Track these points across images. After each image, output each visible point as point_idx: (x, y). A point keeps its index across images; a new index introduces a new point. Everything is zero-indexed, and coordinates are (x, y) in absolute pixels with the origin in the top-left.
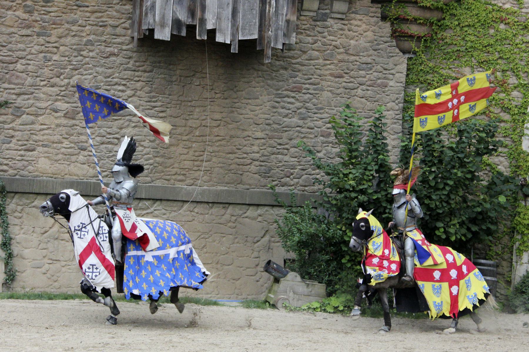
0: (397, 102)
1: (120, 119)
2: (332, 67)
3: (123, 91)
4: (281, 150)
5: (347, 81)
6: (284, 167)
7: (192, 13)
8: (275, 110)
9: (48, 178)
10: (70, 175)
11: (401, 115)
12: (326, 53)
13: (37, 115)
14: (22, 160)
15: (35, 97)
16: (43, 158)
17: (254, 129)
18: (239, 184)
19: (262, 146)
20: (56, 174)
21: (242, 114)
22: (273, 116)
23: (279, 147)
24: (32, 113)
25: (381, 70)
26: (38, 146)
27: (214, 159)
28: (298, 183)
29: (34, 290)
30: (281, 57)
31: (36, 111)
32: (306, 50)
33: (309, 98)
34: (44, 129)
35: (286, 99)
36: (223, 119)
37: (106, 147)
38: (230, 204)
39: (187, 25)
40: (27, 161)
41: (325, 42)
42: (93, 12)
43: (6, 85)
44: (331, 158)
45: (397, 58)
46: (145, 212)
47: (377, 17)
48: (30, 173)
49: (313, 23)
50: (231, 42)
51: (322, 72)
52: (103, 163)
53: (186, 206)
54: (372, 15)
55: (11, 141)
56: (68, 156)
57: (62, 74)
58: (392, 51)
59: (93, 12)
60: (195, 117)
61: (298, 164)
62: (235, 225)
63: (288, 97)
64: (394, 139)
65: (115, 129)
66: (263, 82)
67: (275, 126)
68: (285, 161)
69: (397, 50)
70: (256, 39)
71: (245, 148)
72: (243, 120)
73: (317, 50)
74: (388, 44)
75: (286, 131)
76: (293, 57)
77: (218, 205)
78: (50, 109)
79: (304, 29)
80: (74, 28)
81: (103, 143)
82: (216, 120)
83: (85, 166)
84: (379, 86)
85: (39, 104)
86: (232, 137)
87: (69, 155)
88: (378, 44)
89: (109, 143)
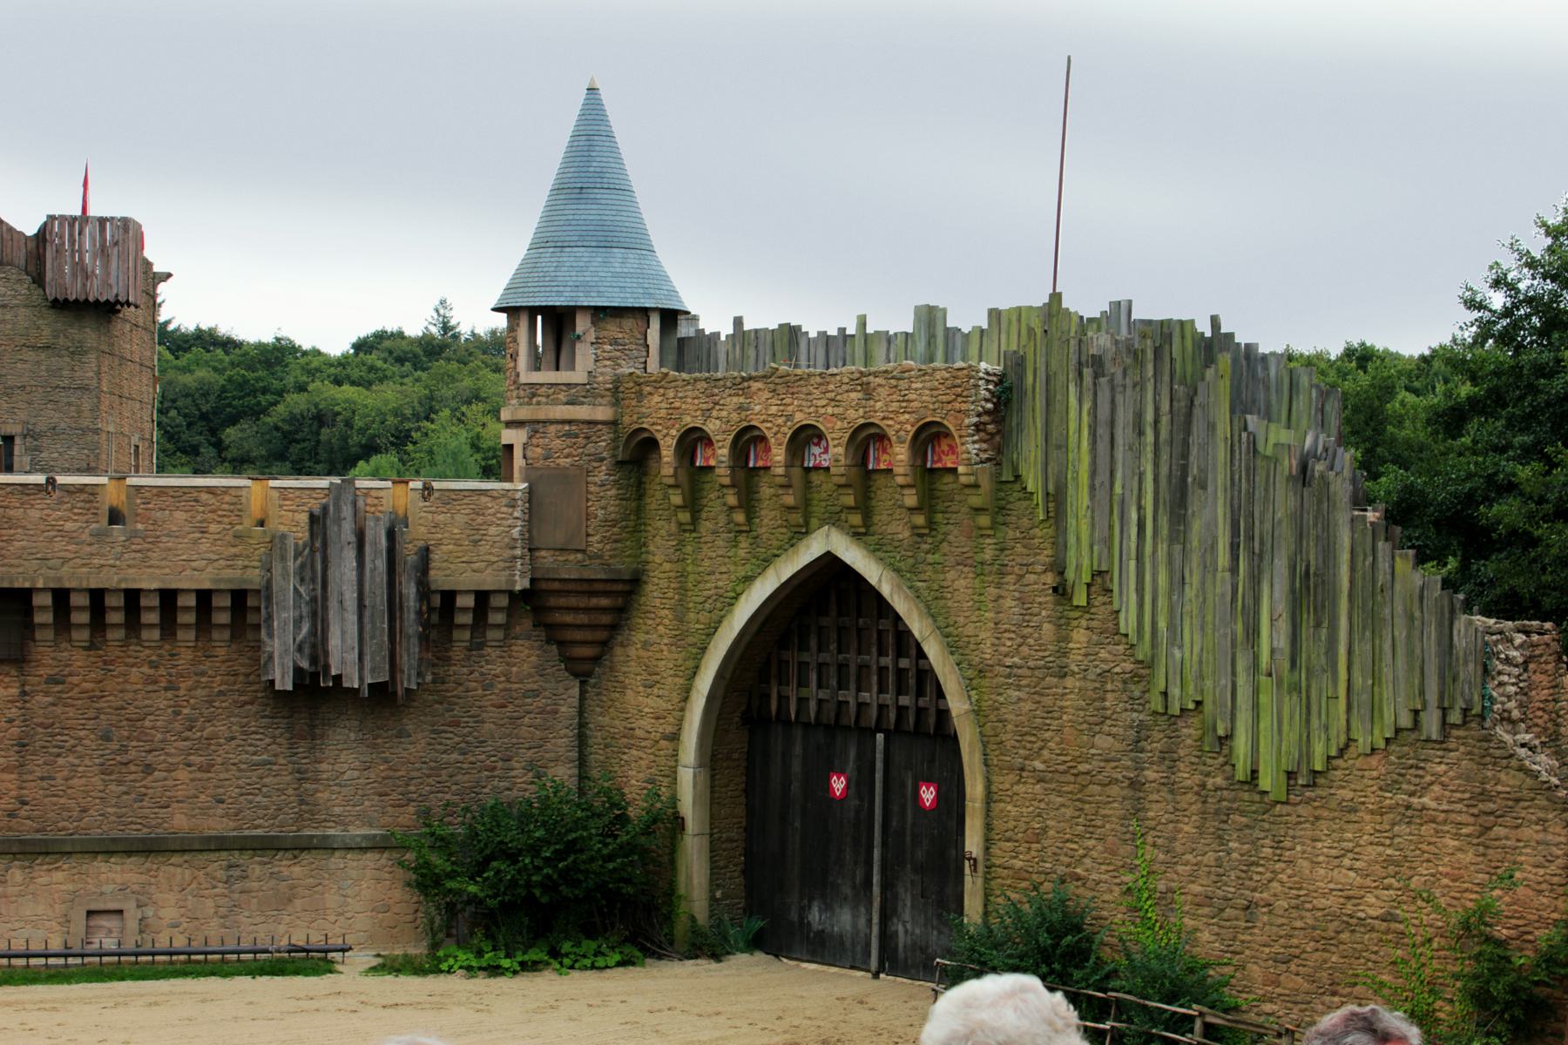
3: (261, 740)
7: (314, 660)
27: (366, 803)
42: (223, 662)
43: (134, 743)
53: (337, 854)
57: (193, 727)
59: (223, 662)
63: (446, 732)
67: (433, 764)
70: (386, 682)
76: (447, 691)
80: (203, 680)
84: (549, 713)
85: (170, 760)
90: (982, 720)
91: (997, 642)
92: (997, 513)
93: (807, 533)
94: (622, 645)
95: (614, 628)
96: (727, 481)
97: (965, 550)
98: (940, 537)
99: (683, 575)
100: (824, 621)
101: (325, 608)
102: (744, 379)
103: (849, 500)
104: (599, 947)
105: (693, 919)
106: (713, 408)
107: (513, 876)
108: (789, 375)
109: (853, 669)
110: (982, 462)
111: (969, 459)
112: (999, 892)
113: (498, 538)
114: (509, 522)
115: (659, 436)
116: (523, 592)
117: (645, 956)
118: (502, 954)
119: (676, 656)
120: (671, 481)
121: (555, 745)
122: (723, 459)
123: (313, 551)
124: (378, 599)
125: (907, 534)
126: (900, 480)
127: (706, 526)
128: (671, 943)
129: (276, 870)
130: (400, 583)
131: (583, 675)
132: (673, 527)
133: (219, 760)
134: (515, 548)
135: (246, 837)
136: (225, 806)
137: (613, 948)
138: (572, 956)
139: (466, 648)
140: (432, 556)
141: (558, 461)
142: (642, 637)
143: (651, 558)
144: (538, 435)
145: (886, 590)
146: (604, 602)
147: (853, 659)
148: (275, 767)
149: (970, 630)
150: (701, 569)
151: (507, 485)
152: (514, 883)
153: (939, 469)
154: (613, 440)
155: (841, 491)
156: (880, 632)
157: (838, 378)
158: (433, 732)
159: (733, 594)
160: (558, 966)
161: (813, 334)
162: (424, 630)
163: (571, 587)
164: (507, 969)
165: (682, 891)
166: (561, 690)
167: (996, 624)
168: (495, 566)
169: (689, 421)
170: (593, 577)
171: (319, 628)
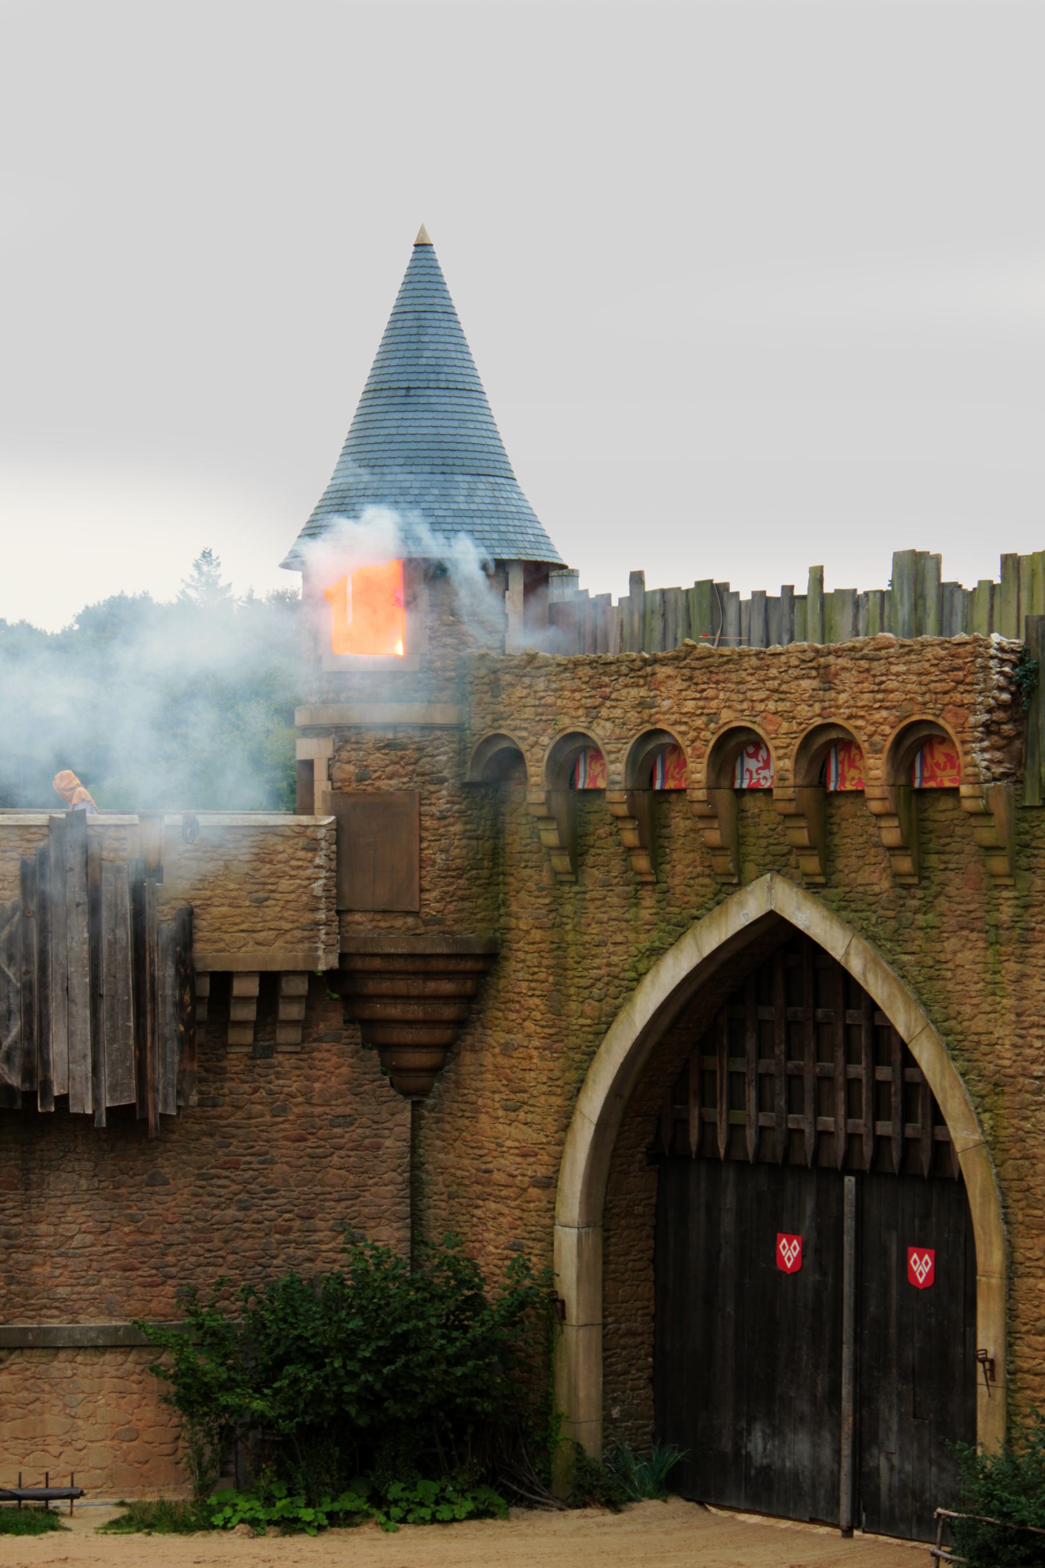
0: (399, 1170)
2: (286, 1126)
5: (314, 1145)
7: (28, 1074)
8: (197, 1199)
11: (408, 1191)
12: (275, 1105)
22: (195, 1208)
25: (370, 1123)
27: (104, 1281)
30: (202, 1118)
32: (240, 1104)
33: (251, 1177)
35: (214, 1181)
39: (23, 1093)
41: (271, 1090)
45: (392, 1104)
47: (356, 1044)
49: (249, 1062)
50: (94, 1111)
51: (270, 1136)
53: (62, 1355)
54: (348, 1041)
58: (385, 1094)
62: (141, 1378)
63: (219, 1177)
64: (398, 1229)
66: (176, 1158)
67: (200, 1224)
69: (392, 1092)
70: (134, 1105)
72: (148, 1218)
73: (261, 1103)
74: (376, 1083)
75: (218, 1230)
77: (114, 1350)
79: (236, 1073)
88: (362, 1085)
90: (1001, 1156)
91: (1020, 1041)
92: (1018, 853)
93: (740, 885)
94: (473, 1050)
95: (461, 1024)
96: (622, 810)
97: (971, 907)
98: (935, 889)
99: (560, 947)
100: (767, 1013)
101: (44, 999)
102: (645, 662)
103: (802, 837)
104: (443, 1490)
105: (579, 1448)
106: (601, 705)
107: (316, 1387)
108: (711, 656)
109: (809, 1083)
110: (995, 779)
111: (975, 775)
112: (1028, 1410)
113: (293, 896)
114: (308, 872)
115: (523, 747)
116: (329, 973)
117: (510, 1504)
118: (301, 1501)
119: (551, 1065)
120: (542, 811)
121: (376, 1195)
122: (618, 778)
123: (26, 917)
124: (121, 985)
125: (885, 884)
126: (875, 806)
127: (593, 875)
128: (548, 1484)
130: (152, 962)
131: (417, 1094)
132: (546, 878)
134: (316, 910)
137: (462, 1492)
138: (403, 1504)
139: (246, 1054)
140: (197, 922)
141: (377, 783)
142: (502, 1037)
143: (513, 922)
144: (349, 747)
145: (856, 967)
146: (447, 987)
147: (809, 1067)
149: (980, 1024)
150: (586, 938)
151: (305, 820)
152: (317, 1396)
153: (932, 790)
154: (461, 752)
155: (788, 824)
156: (847, 1028)
157: (783, 658)
158: (201, 1177)
159: (633, 975)
160: (383, 1519)
161: (745, 596)
162: (187, 1029)
163: (399, 965)
164: (309, 1524)
165: (562, 1408)
166: (385, 1116)
167: (1018, 1015)
168: (288, 936)
169: (569, 724)
170: (428, 951)
171: (36, 1027)
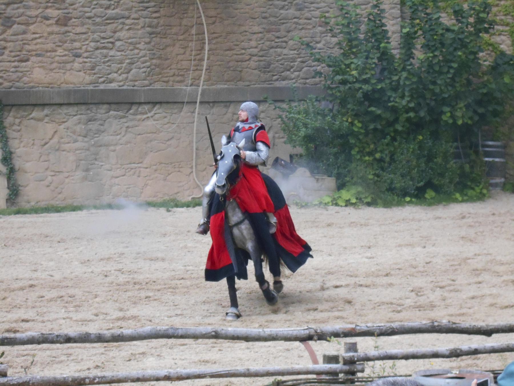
1: (113, 23)
4: (279, 44)
6: (284, 60)
9: (44, 89)
10: (66, 84)
13: (27, 24)
14: (16, 71)
15: (25, 5)
16: (37, 68)
17: (251, 24)
18: (238, 81)
19: (259, 41)
20: (52, 84)
21: (237, 9)
22: (269, 9)
23: (277, 40)
24: (23, 22)
26: (32, 55)
28: (298, 76)
29: (39, 204)
31: (27, 20)
34: (36, 39)
36: (219, 16)
37: (101, 53)
38: (231, 102)
40: (22, 72)
44: (330, 48)
46: (145, 116)
48: (25, 84)
52: (99, 69)
55: (4, 53)
56: (62, 65)
60: (190, 15)
61: (297, 56)
64: (393, 25)
65: (109, 34)
67: (272, 19)
68: (284, 55)
71: (243, 43)
75: (283, 23)
78: (41, 17)
81: (97, 49)
82: (211, 17)
83: (82, 73)
85: (29, 13)
86: (229, 33)
87: (63, 63)
89: (104, 48)
129: (130, 124)
133: (75, 14)
135: (103, 91)
136: (81, 60)
148: (128, 22)
